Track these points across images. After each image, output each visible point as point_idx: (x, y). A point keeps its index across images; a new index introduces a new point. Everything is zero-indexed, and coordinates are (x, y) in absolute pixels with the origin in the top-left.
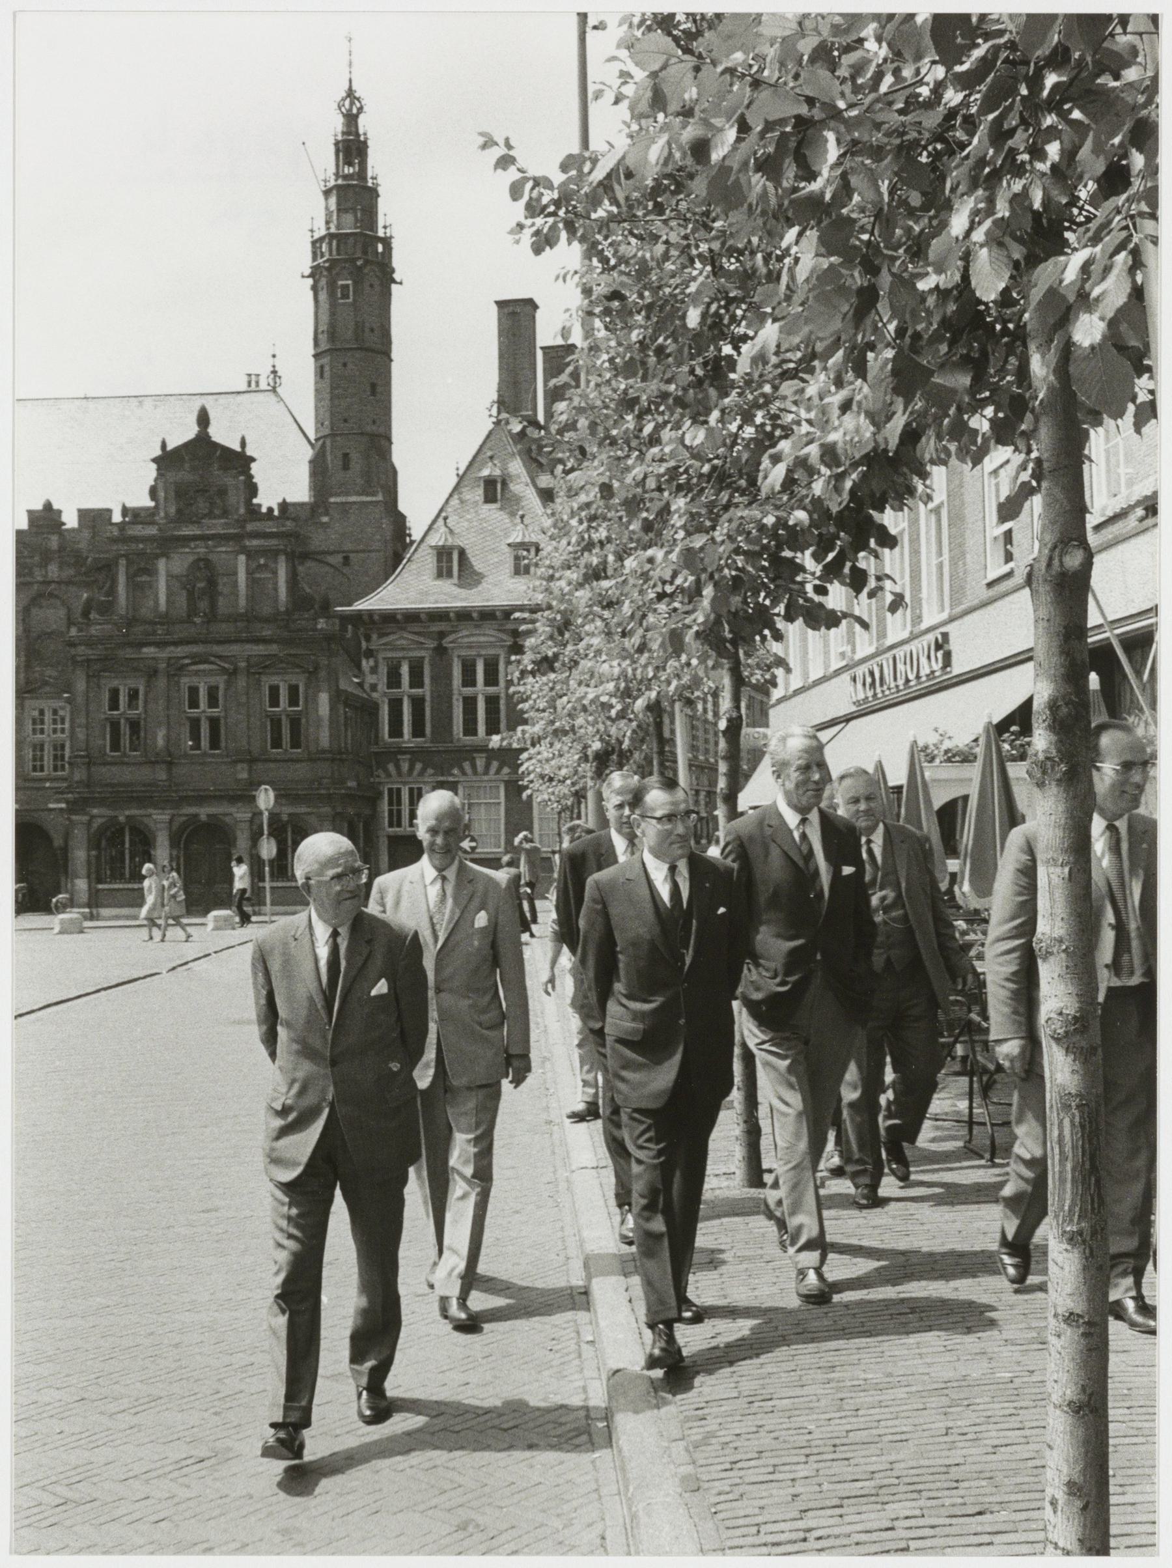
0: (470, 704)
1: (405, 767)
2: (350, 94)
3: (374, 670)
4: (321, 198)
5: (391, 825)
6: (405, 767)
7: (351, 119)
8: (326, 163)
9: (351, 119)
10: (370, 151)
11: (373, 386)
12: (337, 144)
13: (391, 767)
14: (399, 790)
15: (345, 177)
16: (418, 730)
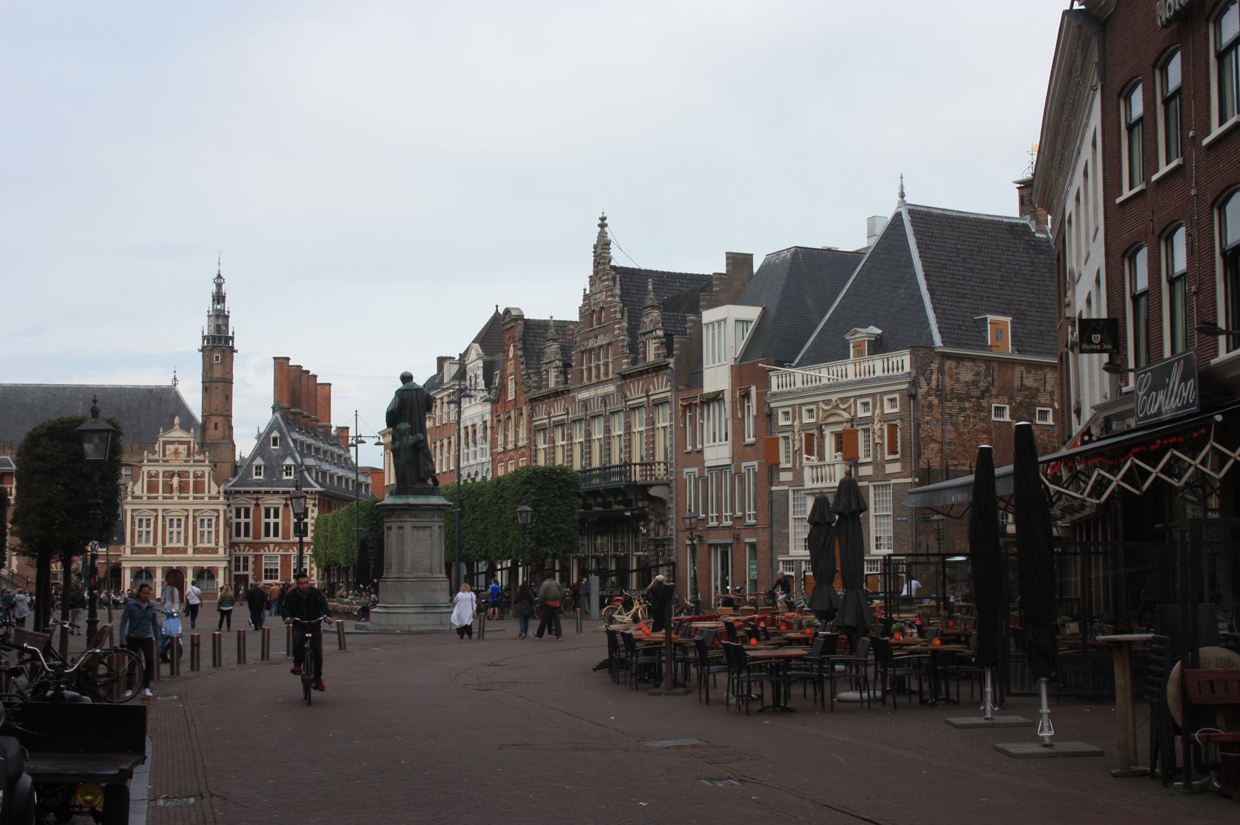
0: (267, 525)
1: (242, 548)
2: (219, 276)
5: (236, 570)
6: (242, 548)
7: (219, 286)
8: (208, 303)
9: (219, 286)
10: (227, 299)
11: (227, 396)
12: (213, 296)
13: (236, 548)
14: (239, 557)
15: (217, 310)
16: (247, 534)
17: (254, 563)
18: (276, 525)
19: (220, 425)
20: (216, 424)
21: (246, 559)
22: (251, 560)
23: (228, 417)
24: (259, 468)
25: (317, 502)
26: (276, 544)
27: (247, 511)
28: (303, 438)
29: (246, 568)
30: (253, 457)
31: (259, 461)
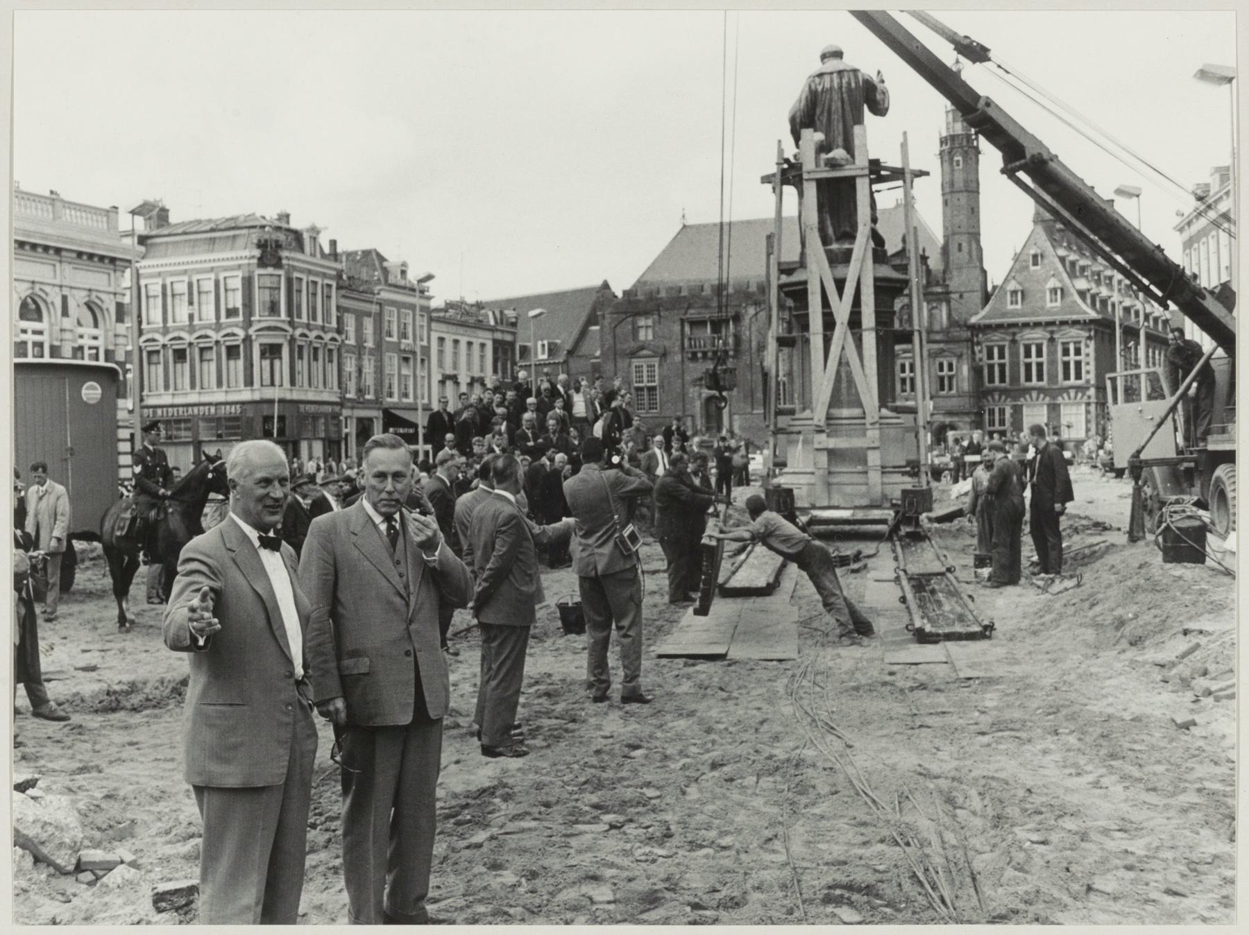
3: (980, 351)
4: (944, 115)
17: (1012, 415)
18: (1040, 365)
19: (964, 245)
20: (960, 245)
21: (1002, 412)
22: (1008, 411)
23: (975, 236)
24: (1014, 293)
25: (1092, 333)
26: (1040, 390)
27: (1001, 350)
28: (1073, 257)
29: (1002, 422)
30: (1006, 280)
31: (1012, 285)
